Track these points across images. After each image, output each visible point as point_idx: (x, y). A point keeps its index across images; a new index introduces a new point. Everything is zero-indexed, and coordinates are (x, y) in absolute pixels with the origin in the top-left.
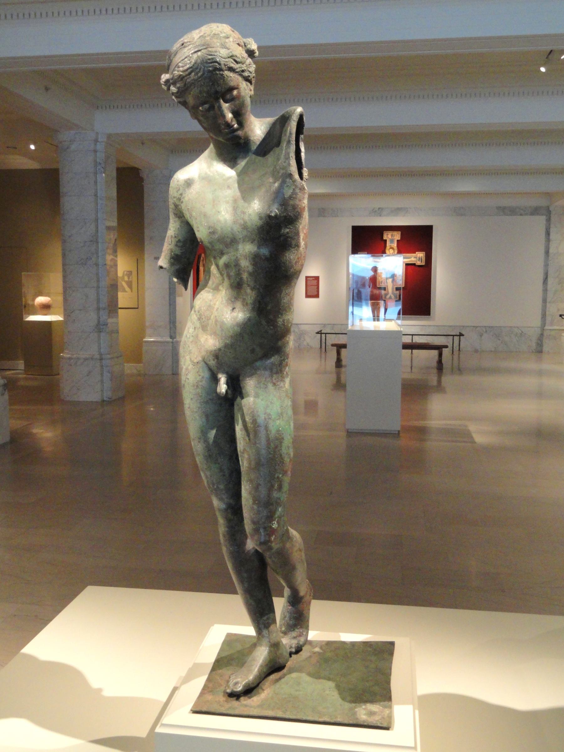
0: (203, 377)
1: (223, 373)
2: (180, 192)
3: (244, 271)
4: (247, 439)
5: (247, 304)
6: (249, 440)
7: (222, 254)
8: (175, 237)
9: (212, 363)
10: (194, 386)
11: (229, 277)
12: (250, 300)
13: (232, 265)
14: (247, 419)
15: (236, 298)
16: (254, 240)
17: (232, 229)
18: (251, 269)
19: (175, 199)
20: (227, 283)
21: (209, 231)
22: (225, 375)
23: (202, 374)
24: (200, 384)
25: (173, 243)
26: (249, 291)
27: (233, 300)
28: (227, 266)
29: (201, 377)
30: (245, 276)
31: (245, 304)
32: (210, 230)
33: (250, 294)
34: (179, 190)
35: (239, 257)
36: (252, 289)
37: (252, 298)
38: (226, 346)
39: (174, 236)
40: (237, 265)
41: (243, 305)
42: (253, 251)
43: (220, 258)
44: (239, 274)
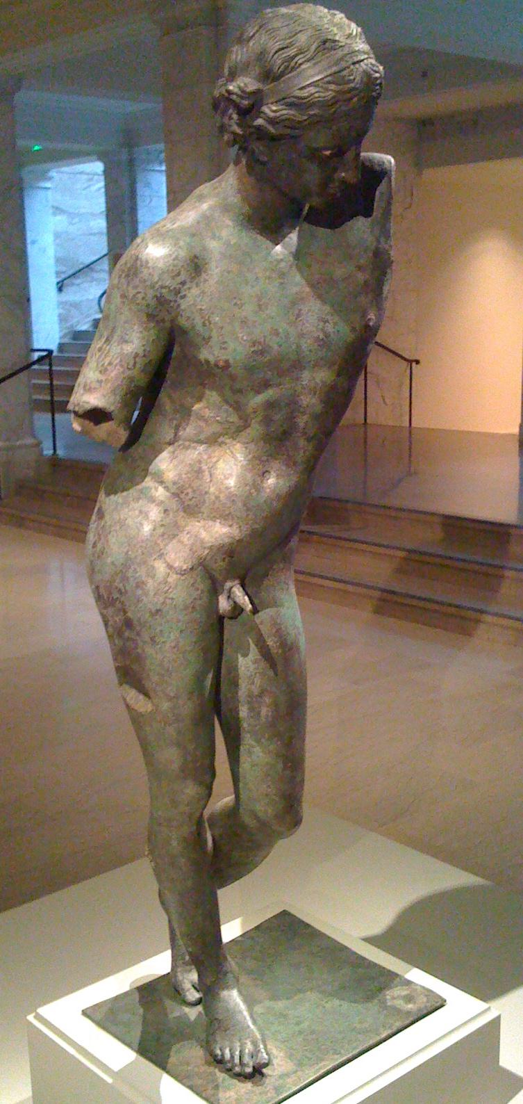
0: (202, 592)
1: (234, 578)
2: (179, 279)
3: (304, 413)
4: (271, 673)
5: (295, 464)
6: (276, 674)
7: (266, 385)
8: (144, 356)
9: (220, 565)
10: (186, 608)
11: (267, 421)
12: (300, 456)
13: (283, 404)
14: (271, 642)
15: (272, 456)
16: (333, 364)
17: (299, 346)
18: (318, 408)
19: (164, 291)
20: (255, 429)
21: (252, 349)
22: (237, 582)
23: (201, 587)
24: (199, 602)
25: (138, 366)
26: (302, 442)
27: (264, 458)
28: (270, 405)
29: (199, 592)
30: (302, 421)
31: (290, 462)
32: (256, 348)
33: (303, 449)
34: (179, 274)
35: (299, 389)
36: (309, 440)
37: (307, 453)
38: (254, 534)
39: (141, 353)
40: (293, 403)
41: (288, 465)
42: (329, 382)
43: (258, 392)
44: (291, 418)
